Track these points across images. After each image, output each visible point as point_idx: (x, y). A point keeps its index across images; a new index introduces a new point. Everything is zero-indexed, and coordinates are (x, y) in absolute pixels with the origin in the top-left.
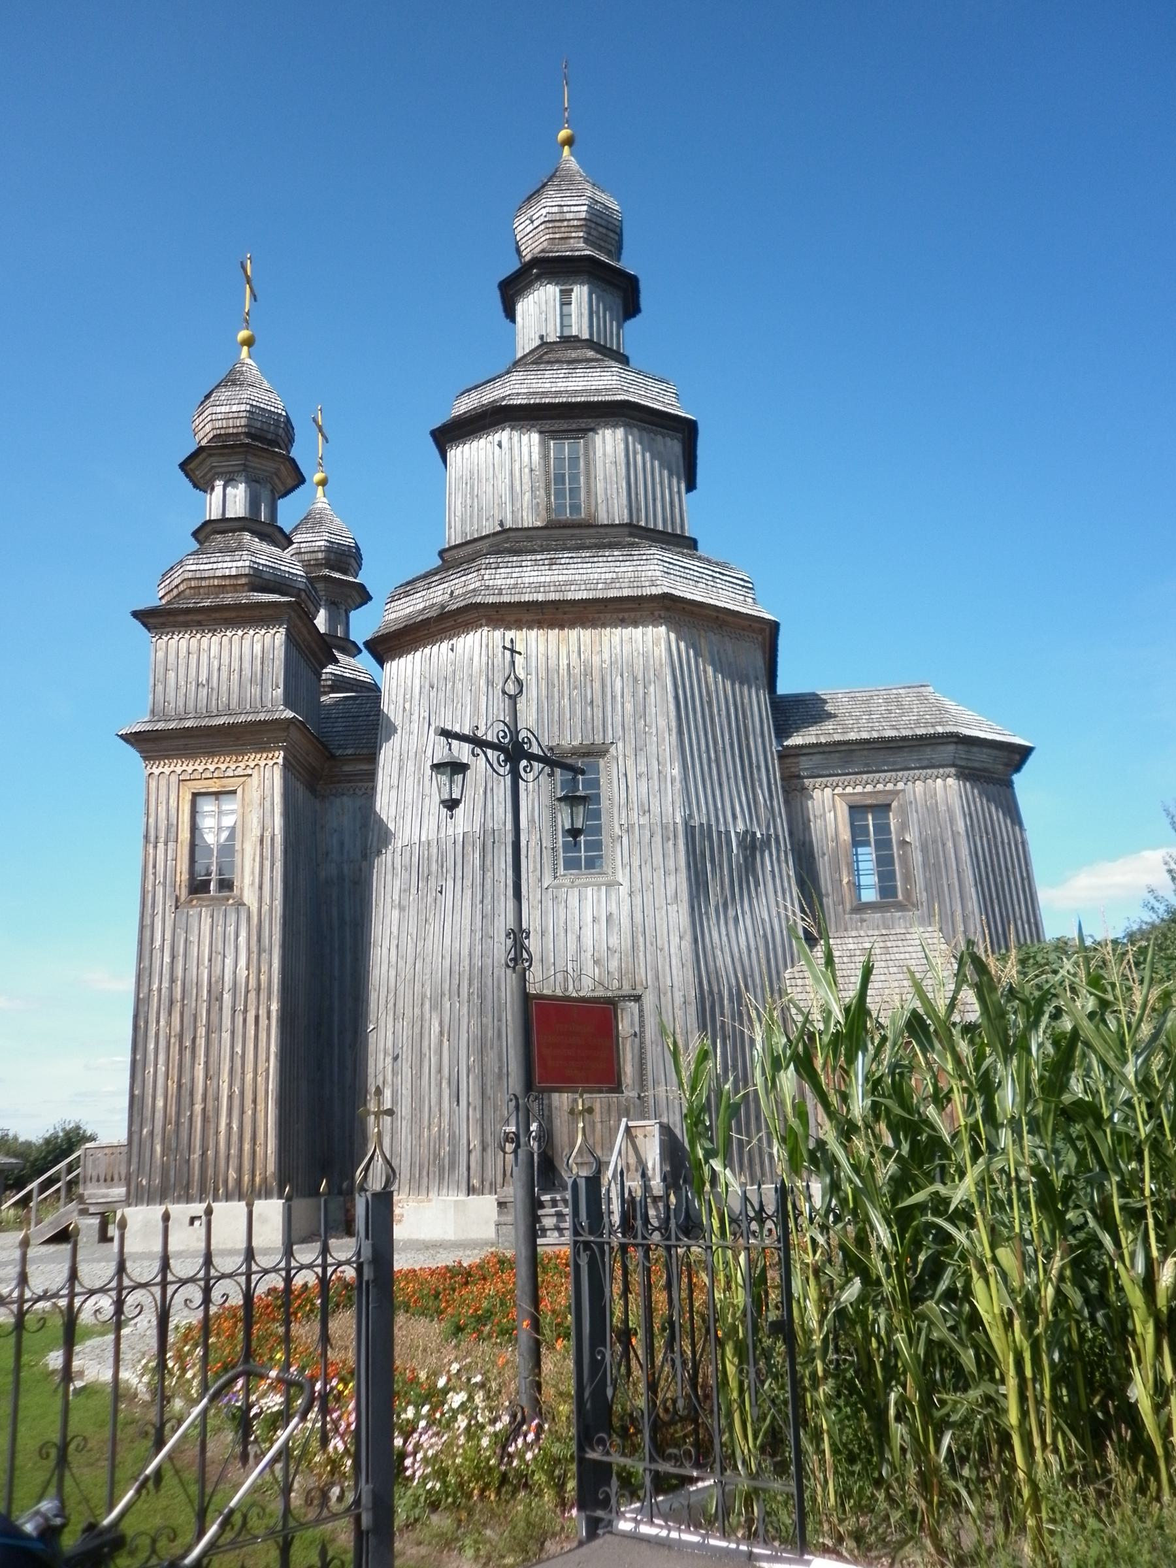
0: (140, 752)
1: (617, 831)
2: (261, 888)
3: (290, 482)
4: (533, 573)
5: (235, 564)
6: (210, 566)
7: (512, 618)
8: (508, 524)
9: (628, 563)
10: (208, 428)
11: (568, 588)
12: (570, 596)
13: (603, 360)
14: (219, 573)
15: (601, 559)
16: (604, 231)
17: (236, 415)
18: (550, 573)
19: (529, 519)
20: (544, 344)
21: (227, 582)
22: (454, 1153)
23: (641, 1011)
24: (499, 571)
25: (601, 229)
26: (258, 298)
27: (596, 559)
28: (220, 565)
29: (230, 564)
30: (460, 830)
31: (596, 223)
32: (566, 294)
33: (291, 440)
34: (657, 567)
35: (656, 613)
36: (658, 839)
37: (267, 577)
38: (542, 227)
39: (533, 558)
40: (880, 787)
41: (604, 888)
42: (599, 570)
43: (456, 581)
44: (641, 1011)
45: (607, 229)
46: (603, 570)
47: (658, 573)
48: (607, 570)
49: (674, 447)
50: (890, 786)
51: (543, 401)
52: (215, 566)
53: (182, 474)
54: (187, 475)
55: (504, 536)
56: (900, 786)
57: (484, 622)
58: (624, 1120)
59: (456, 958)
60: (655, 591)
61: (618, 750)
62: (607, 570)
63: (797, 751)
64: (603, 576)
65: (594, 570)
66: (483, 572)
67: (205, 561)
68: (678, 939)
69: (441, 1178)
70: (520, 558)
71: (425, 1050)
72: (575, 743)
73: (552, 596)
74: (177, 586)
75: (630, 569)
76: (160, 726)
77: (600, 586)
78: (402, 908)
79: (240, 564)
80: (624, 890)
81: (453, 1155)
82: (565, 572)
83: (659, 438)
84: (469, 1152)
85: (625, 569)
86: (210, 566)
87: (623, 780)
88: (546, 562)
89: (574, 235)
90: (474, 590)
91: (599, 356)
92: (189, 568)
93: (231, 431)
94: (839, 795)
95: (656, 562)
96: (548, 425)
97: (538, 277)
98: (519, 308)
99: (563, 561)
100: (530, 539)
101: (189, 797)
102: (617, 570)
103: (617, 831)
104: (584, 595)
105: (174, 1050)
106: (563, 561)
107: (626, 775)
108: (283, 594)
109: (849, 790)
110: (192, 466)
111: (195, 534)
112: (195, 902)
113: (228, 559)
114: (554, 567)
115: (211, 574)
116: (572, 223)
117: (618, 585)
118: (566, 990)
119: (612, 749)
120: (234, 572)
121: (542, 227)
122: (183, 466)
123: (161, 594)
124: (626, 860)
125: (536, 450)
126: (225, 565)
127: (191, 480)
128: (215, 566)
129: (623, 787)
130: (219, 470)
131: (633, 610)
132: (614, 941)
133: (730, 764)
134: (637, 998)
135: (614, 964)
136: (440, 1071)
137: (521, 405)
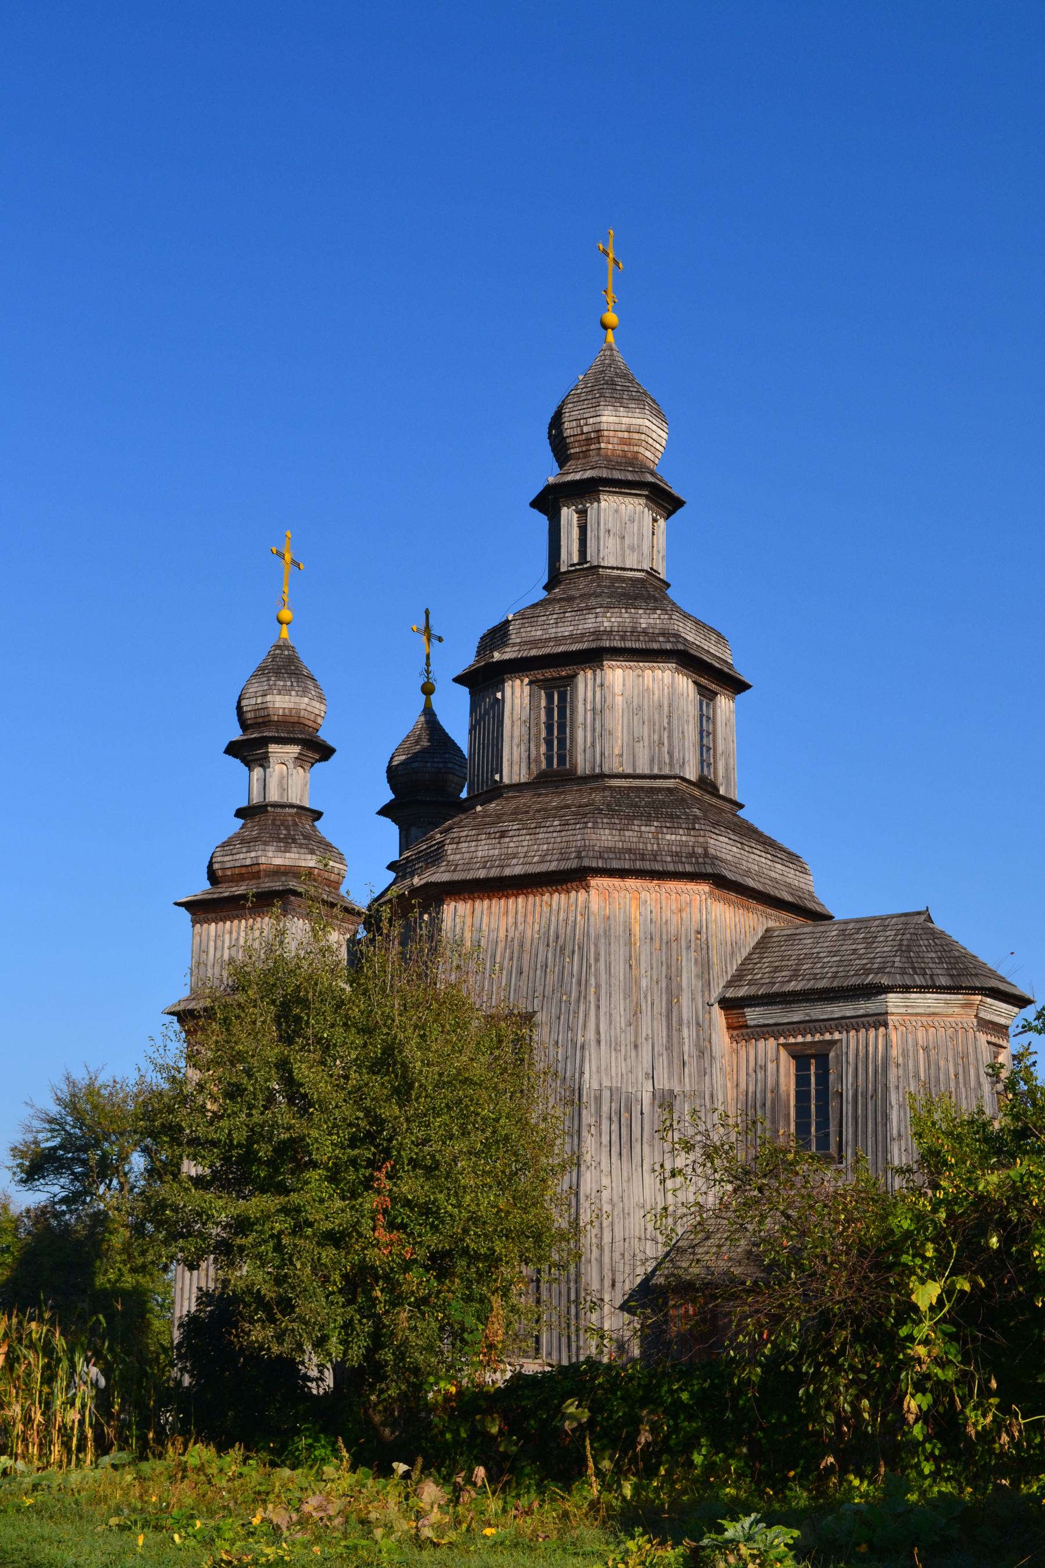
4: (486, 847)
12: (507, 872)
16: (626, 435)
17: (260, 706)
21: (244, 871)
25: (620, 434)
32: (583, 513)
40: (818, 1037)
50: (828, 1037)
56: (837, 1036)
73: (494, 873)
89: (593, 447)
94: (784, 1045)
104: (518, 870)
106: (511, 833)
109: (792, 1040)
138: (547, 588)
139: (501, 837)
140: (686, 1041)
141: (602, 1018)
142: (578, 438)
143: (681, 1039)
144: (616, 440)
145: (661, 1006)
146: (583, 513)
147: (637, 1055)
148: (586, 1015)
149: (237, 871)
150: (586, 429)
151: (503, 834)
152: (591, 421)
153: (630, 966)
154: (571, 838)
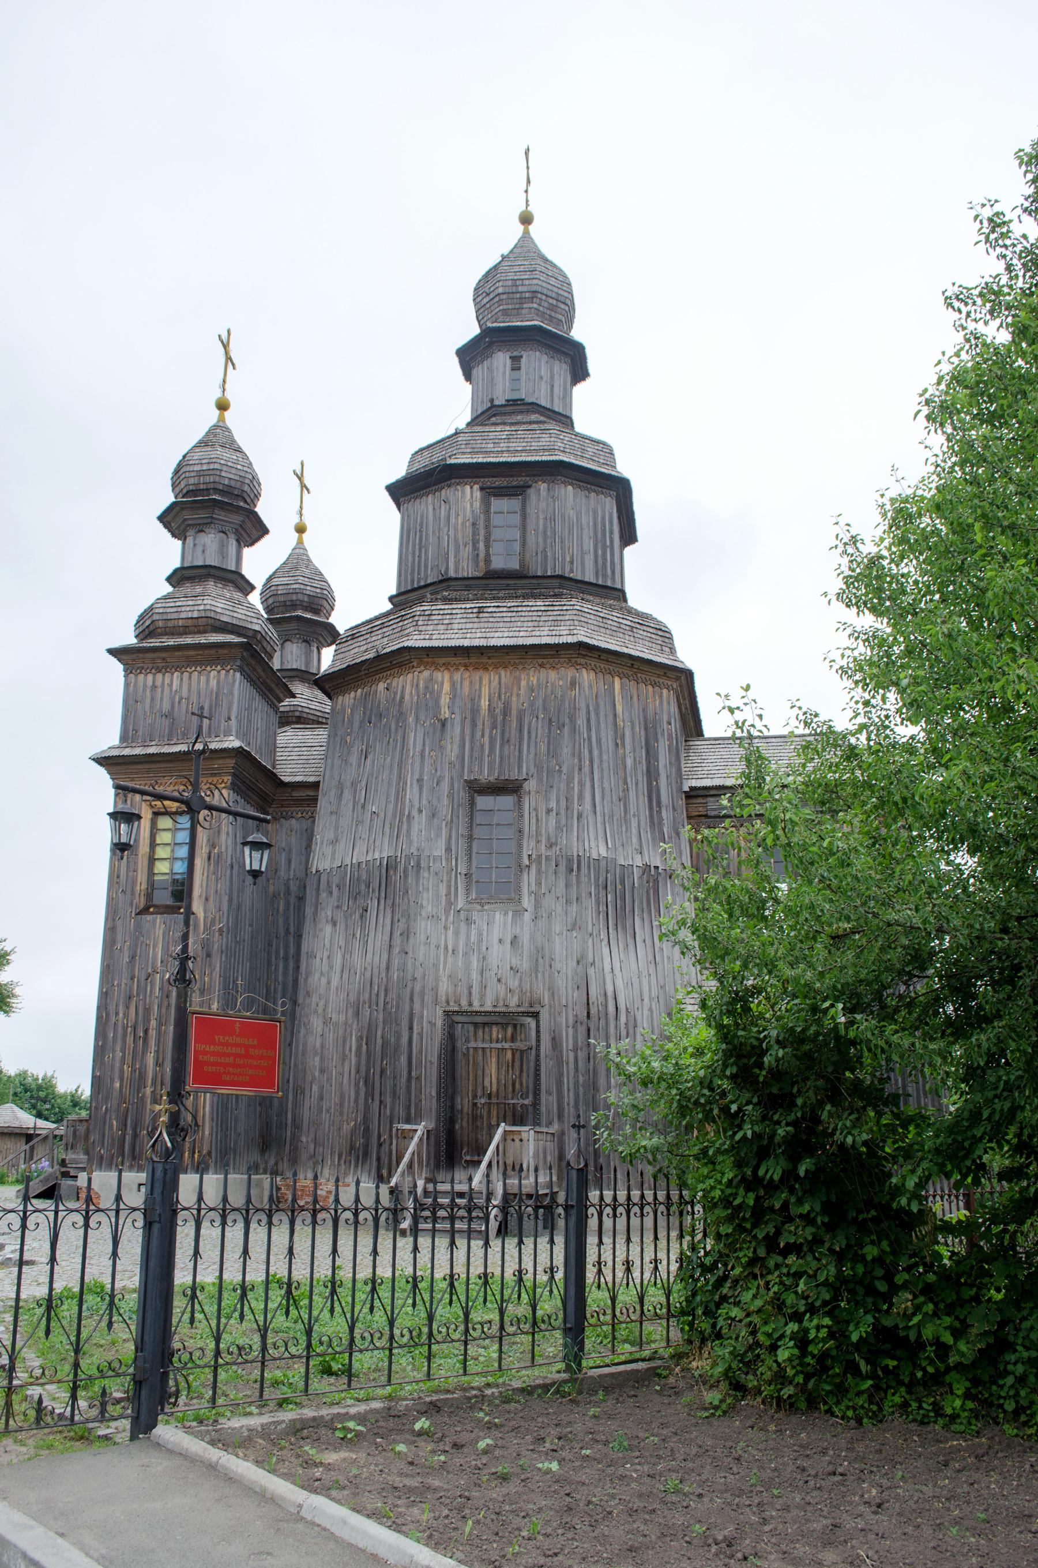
0: (109, 773)
1: (526, 862)
2: (207, 899)
3: (255, 534)
5: (196, 608)
6: (175, 610)
7: (442, 661)
8: (452, 574)
9: (549, 613)
10: (183, 485)
11: (492, 635)
13: (544, 422)
14: (183, 616)
15: (524, 609)
16: (554, 302)
18: (476, 620)
19: (467, 570)
20: (493, 406)
22: (368, 1145)
23: (538, 1026)
24: (433, 617)
25: (551, 301)
26: (237, 366)
27: (520, 609)
28: (183, 609)
29: (192, 608)
30: (385, 855)
31: (547, 296)
32: (516, 360)
33: (257, 496)
34: (575, 618)
35: (573, 660)
36: (562, 868)
37: (225, 619)
38: (497, 299)
39: (463, 606)
41: (510, 914)
42: (522, 619)
43: (394, 626)
44: (538, 1026)
45: (557, 300)
46: (526, 619)
47: (576, 623)
48: (530, 619)
49: (609, 505)
51: (485, 460)
52: (179, 609)
53: (160, 526)
54: (166, 527)
55: (445, 584)
57: (415, 664)
58: (503, 1124)
59: (376, 971)
60: (570, 640)
61: (531, 785)
62: (530, 619)
63: (705, 793)
64: (525, 624)
65: (517, 619)
66: (416, 618)
67: (172, 604)
68: (575, 963)
69: (356, 1166)
70: (450, 607)
71: (347, 1052)
72: (492, 779)
74: (148, 627)
75: (551, 618)
76: (127, 752)
77: (521, 634)
78: (334, 924)
79: (202, 608)
80: (527, 917)
81: (366, 1147)
82: (491, 620)
83: (593, 494)
84: (380, 1145)
85: (546, 618)
86: (175, 610)
87: (533, 814)
88: (475, 610)
89: (525, 306)
90: (408, 635)
91: (542, 418)
92: (157, 611)
93: (202, 487)
95: (574, 612)
96: (489, 482)
97: (491, 344)
98: (474, 372)
99: (490, 610)
100: (468, 588)
101: (150, 816)
102: (538, 619)
103: (526, 862)
105: (130, 1040)
106: (490, 610)
107: (536, 809)
108: (239, 635)
110: (169, 518)
111: (169, 579)
112: (151, 910)
113: (191, 603)
114: (481, 615)
115: (175, 616)
116: (524, 295)
117: (538, 633)
118: (470, 1005)
119: (526, 786)
120: (195, 615)
121: (497, 299)
122: (161, 518)
123: (138, 632)
124: (533, 888)
125: (477, 505)
126: (188, 609)
127: (169, 531)
128: (179, 609)
129: (533, 821)
130: (190, 522)
131: (552, 656)
132: (515, 962)
133: (638, 802)
134: (536, 1015)
135: (514, 984)
136: (358, 1071)
137: (464, 464)
138: (468, 424)
139: (479, 612)
140: (665, 822)
141: (596, 790)
142: (511, 296)
143: (661, 819)
144: (546, 305)
145: (643, 786)
146: (516, 360)
147: (627, 831)
148: (581, 785)
149: (181, 623)
150: (520, 289)
151: (481, 609)
152: (527, 282)
153: (617, 744)
154: (559, 618)
